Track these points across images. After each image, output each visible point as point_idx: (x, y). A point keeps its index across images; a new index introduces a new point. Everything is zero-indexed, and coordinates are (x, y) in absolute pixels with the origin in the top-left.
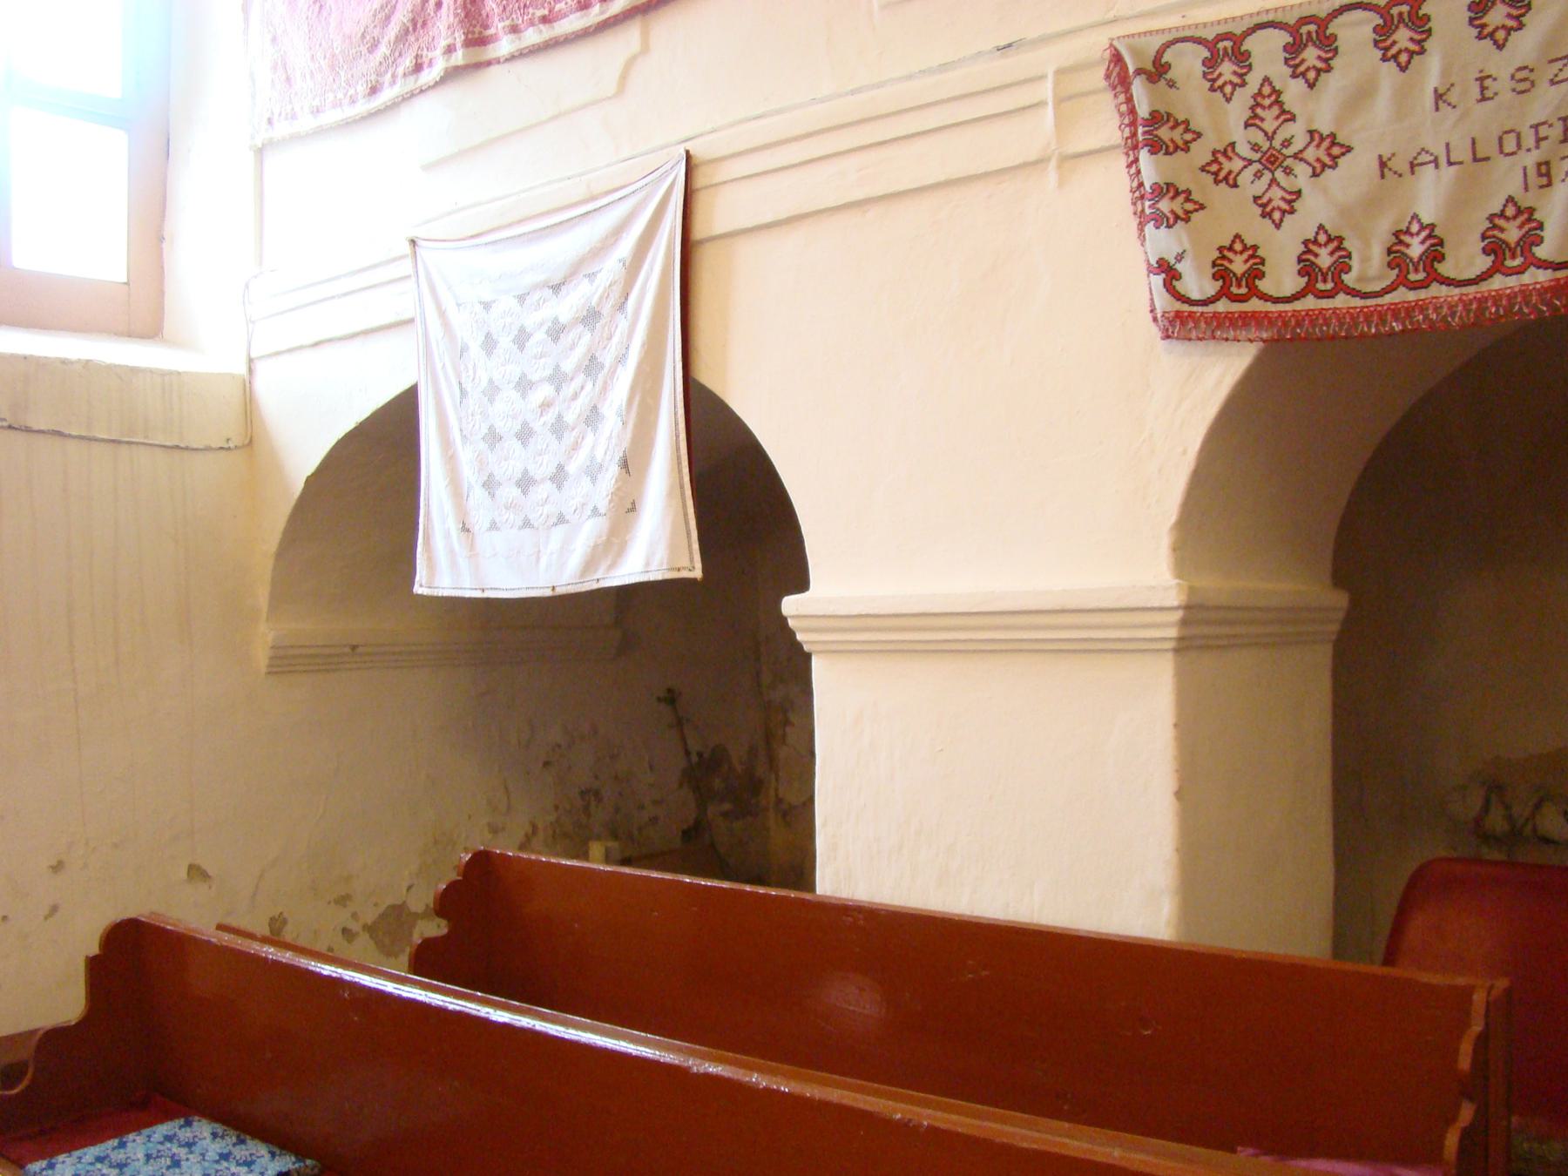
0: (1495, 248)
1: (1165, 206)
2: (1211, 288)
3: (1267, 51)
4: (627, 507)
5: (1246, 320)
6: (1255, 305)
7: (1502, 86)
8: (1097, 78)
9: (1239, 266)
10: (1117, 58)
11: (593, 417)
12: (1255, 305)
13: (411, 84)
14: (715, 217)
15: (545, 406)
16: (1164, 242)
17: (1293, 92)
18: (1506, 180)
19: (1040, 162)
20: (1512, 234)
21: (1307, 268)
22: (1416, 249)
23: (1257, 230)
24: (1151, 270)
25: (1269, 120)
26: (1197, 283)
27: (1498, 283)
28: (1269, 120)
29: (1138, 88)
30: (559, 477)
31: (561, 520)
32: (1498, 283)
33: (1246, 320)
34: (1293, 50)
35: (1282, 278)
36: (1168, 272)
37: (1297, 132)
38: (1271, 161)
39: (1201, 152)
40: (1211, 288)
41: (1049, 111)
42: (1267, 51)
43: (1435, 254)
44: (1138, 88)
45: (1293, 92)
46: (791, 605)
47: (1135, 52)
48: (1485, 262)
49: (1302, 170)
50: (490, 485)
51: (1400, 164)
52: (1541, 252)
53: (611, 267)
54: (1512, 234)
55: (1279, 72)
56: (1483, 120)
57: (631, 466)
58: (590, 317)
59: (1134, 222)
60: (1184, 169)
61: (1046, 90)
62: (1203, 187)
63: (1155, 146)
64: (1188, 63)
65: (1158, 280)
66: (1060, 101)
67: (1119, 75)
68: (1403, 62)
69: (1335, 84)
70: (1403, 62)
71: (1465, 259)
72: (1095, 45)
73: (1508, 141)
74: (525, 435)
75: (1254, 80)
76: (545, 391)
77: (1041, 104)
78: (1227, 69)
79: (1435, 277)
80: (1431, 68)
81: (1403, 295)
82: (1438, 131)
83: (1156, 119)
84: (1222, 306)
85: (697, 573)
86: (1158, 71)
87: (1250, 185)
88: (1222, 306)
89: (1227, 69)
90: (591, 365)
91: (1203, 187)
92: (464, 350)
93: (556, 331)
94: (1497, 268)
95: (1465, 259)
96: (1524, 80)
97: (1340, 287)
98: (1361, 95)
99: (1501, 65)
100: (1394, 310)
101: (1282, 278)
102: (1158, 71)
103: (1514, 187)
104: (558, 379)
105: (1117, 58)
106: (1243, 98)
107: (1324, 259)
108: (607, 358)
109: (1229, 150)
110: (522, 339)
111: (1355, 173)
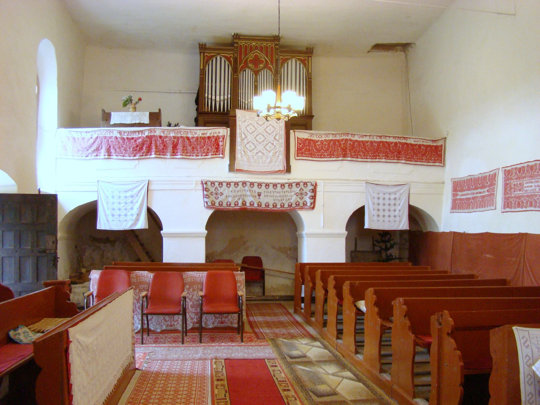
0: (235, 205)
1: (207, 197)
2: (211, 205)
3: (217, 184)
4: (137, 220)
5: (214, 208)
6: (215, 207)
7: (236, 191)
8: (200, 182)
9: (213, 203)
10: (202, 181)
11: (132, 209)
12: (215, 207)
13: (95, 157)
14: (152, 187)
15: (124, 206)
16: (206, 200)
17: (219, 188)
18: (236, 199)
19: (193, 189)
20: (236, 203)
21: (219, 204)
22: (229, 203)
23: (215, 200)
24: (204, 202)
25: (216, 190)
26: (209, 204)
27: (235, 207)
28: (216, 190)
29: (204, 185)
30: (126, 215)
31: (126, 220)
32: (235, 207)
33: (214, 208)
34: (219, 184)
35: (217, 204)
36: (207, 203)
37: (219, 192)
38: (217, 194)
39: (210, 192)
40: (211, 205)
41: (194, 185)
42: (217, 184)
43: (230, 204)
44: (204, 185)
45: (219, 188)
46: (162, 232)
47: (204, 181)
48: (234, 205)
49: (219, 195)
50: (113, 215)
51: (228, 196)
52: (239, 205)
53: (135, 191)
54: (236, 203)
55: (218, 186)
56: (235, 194)
57: (138, 215)
58: (132, 196)
59: (203, 197)
60: (208, 193)
61: (194, 182)
62: (210, 195)
63: (206, 191)
64: (209, 183)
65: (205, 203)
66: (195, 184)
67: (202, 183)
68: (229, 188)
69: (223, 188)
70: (229, 188)
71: (233, 205)
72: (200, 179)
73: (236, 196)
74: (120, 209)
75: (215, 186)
76: (124, 204)
77: (193, 184)
78: (213, 185)
79: (230, 206)
80: (231, 189)
81: (227, 207)
82: (231, 194)
83: (206, 188)
84: (212, 206)
85: (148, 228)
86: (206, 183)
87: (214, 196)
88: (212, 206)
89: (213, 185)
90: (132, 202)
91: (210, 195)
92: (108, 197)
93: (126, 197)
94: (235, 206)
95: (233, 205)
96: (238, 191)
97: (222, 206)
98: (225, 190)
99: (236, 190)
100: (227, 209)
101: (217, 204)
102: (206, 183)
103: (237, 200)
104: (126, 203)
105: (202, 181)
106: (214, 188)
107: (221, 203)
108: (135, 201)
109: (213, 192)
110: (119, 197)
111: (224, 196)
